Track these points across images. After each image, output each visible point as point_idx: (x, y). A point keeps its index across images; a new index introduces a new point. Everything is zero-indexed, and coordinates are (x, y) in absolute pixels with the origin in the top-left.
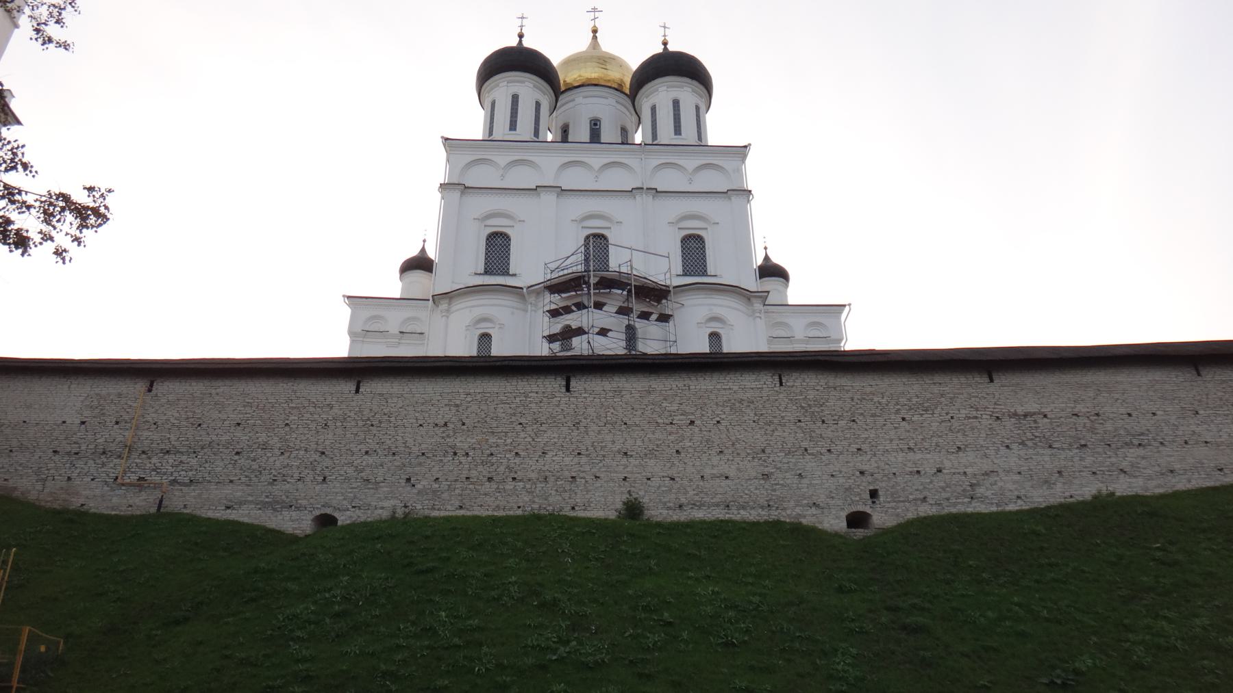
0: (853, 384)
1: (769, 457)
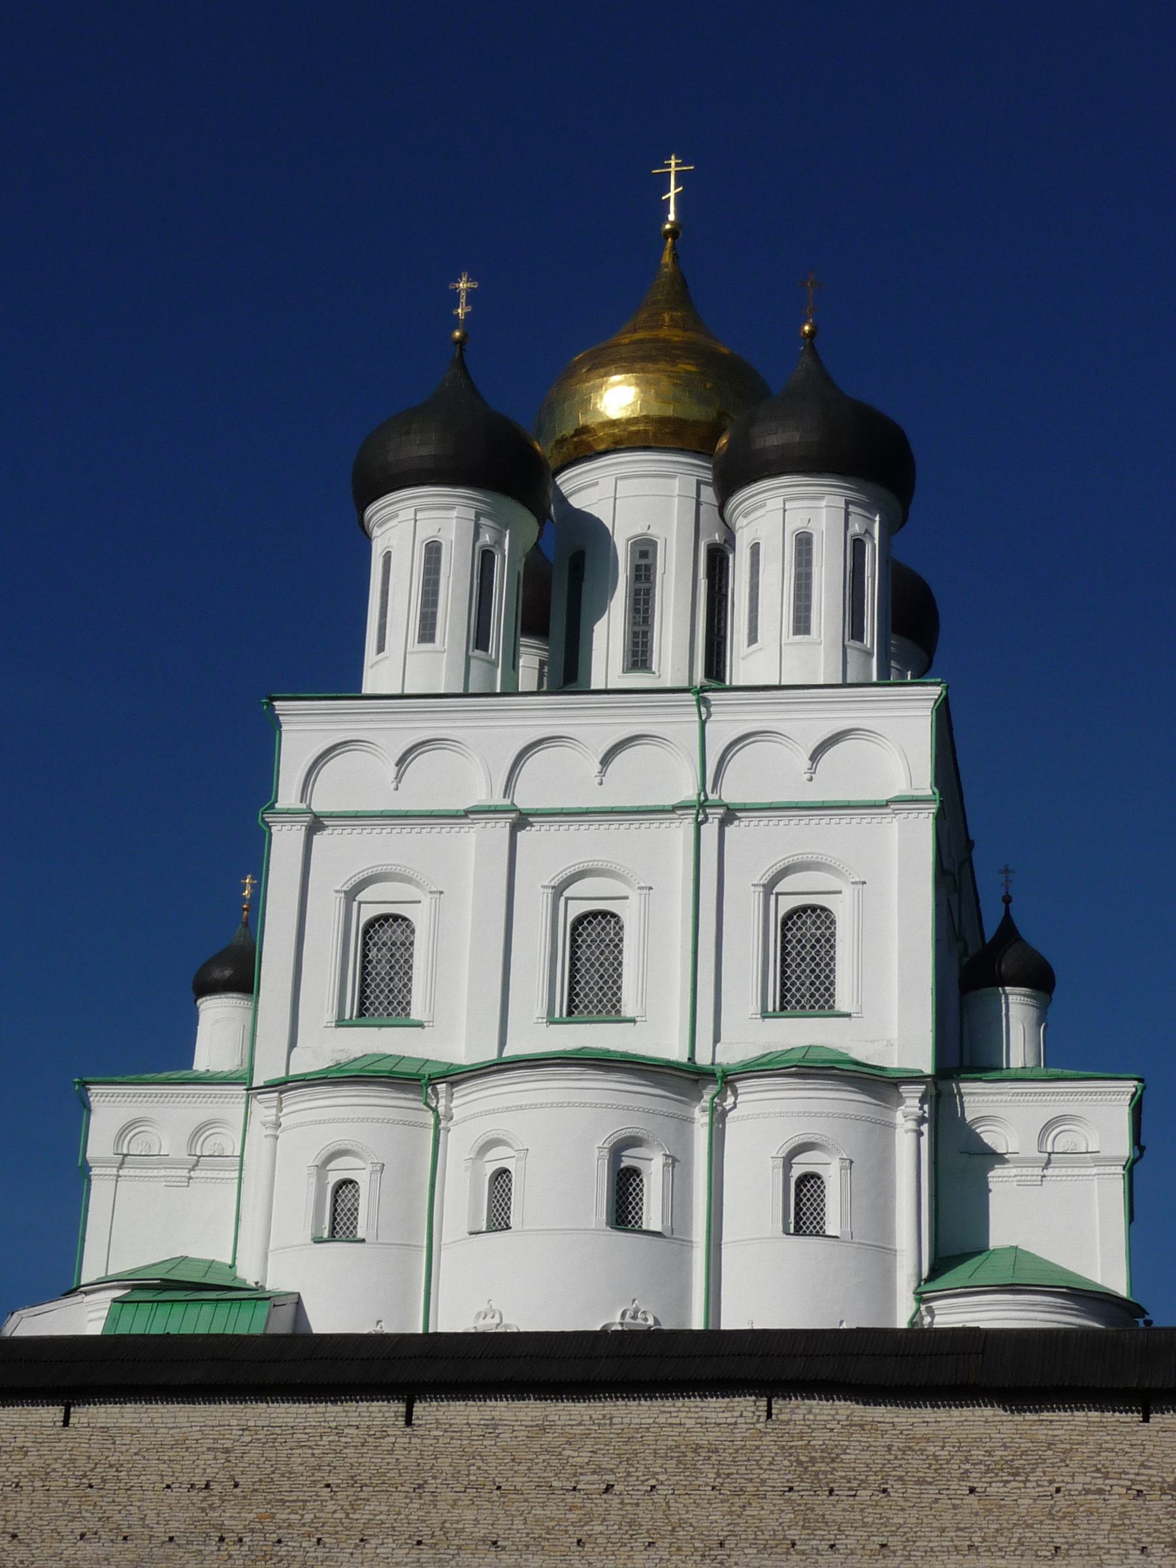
1: (729, 1556)
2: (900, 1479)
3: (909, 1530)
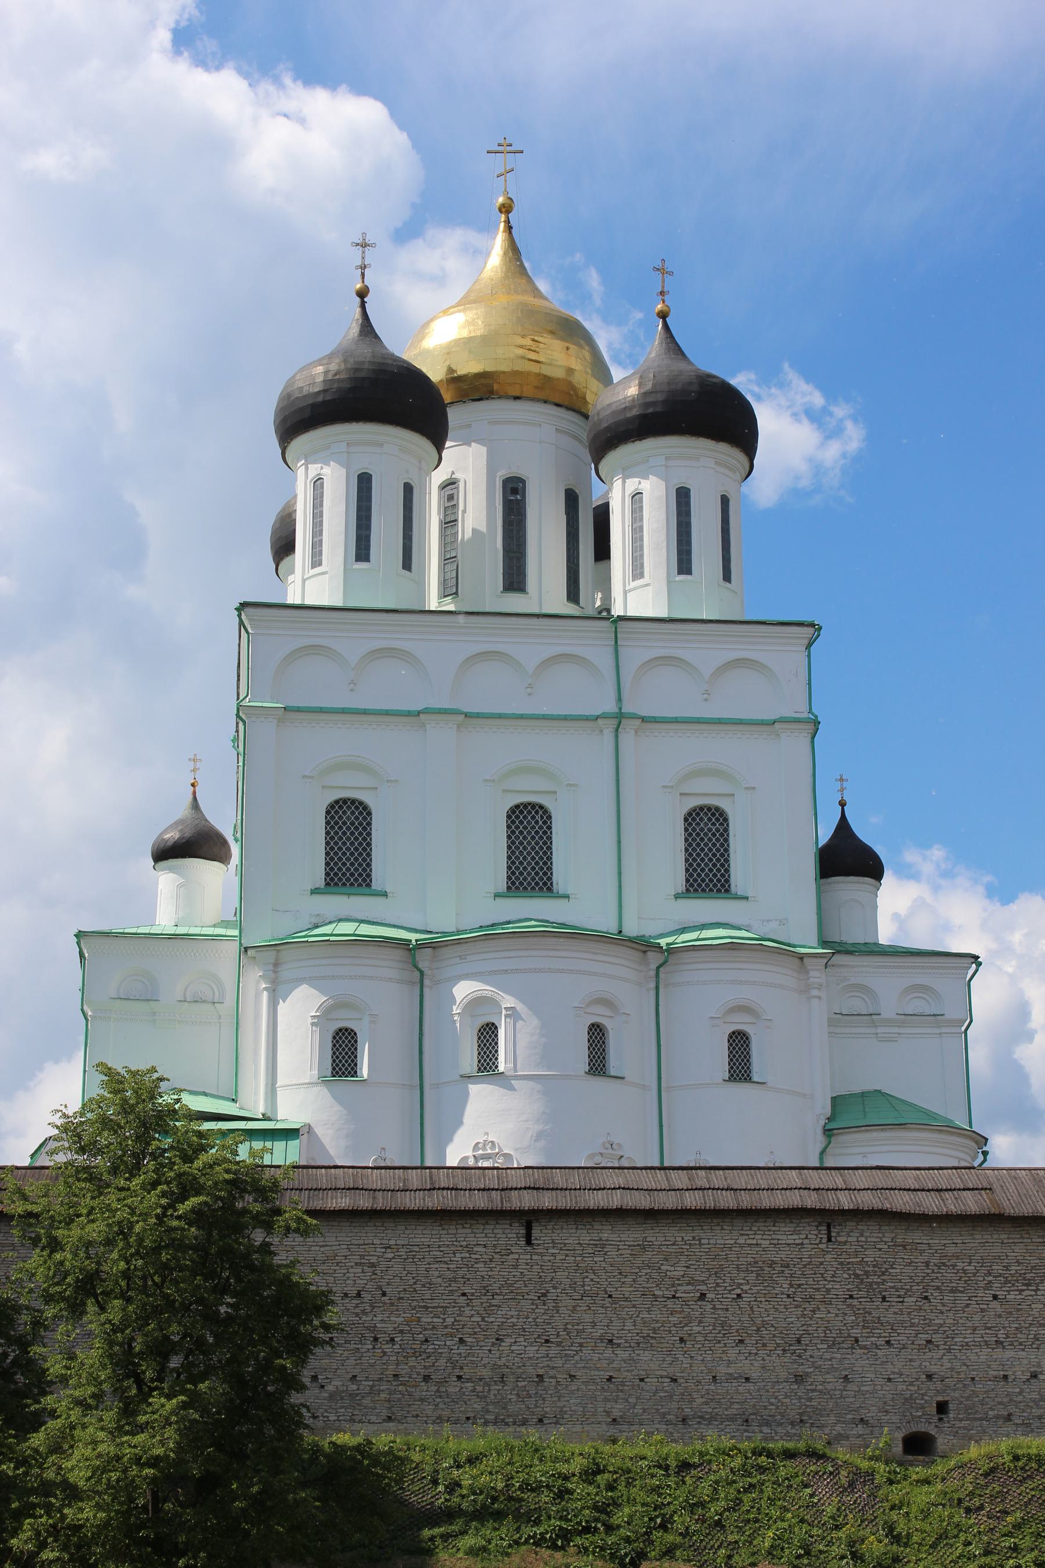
0: (931, 1241)
1: (805, 1350)
3: (948, 1329)
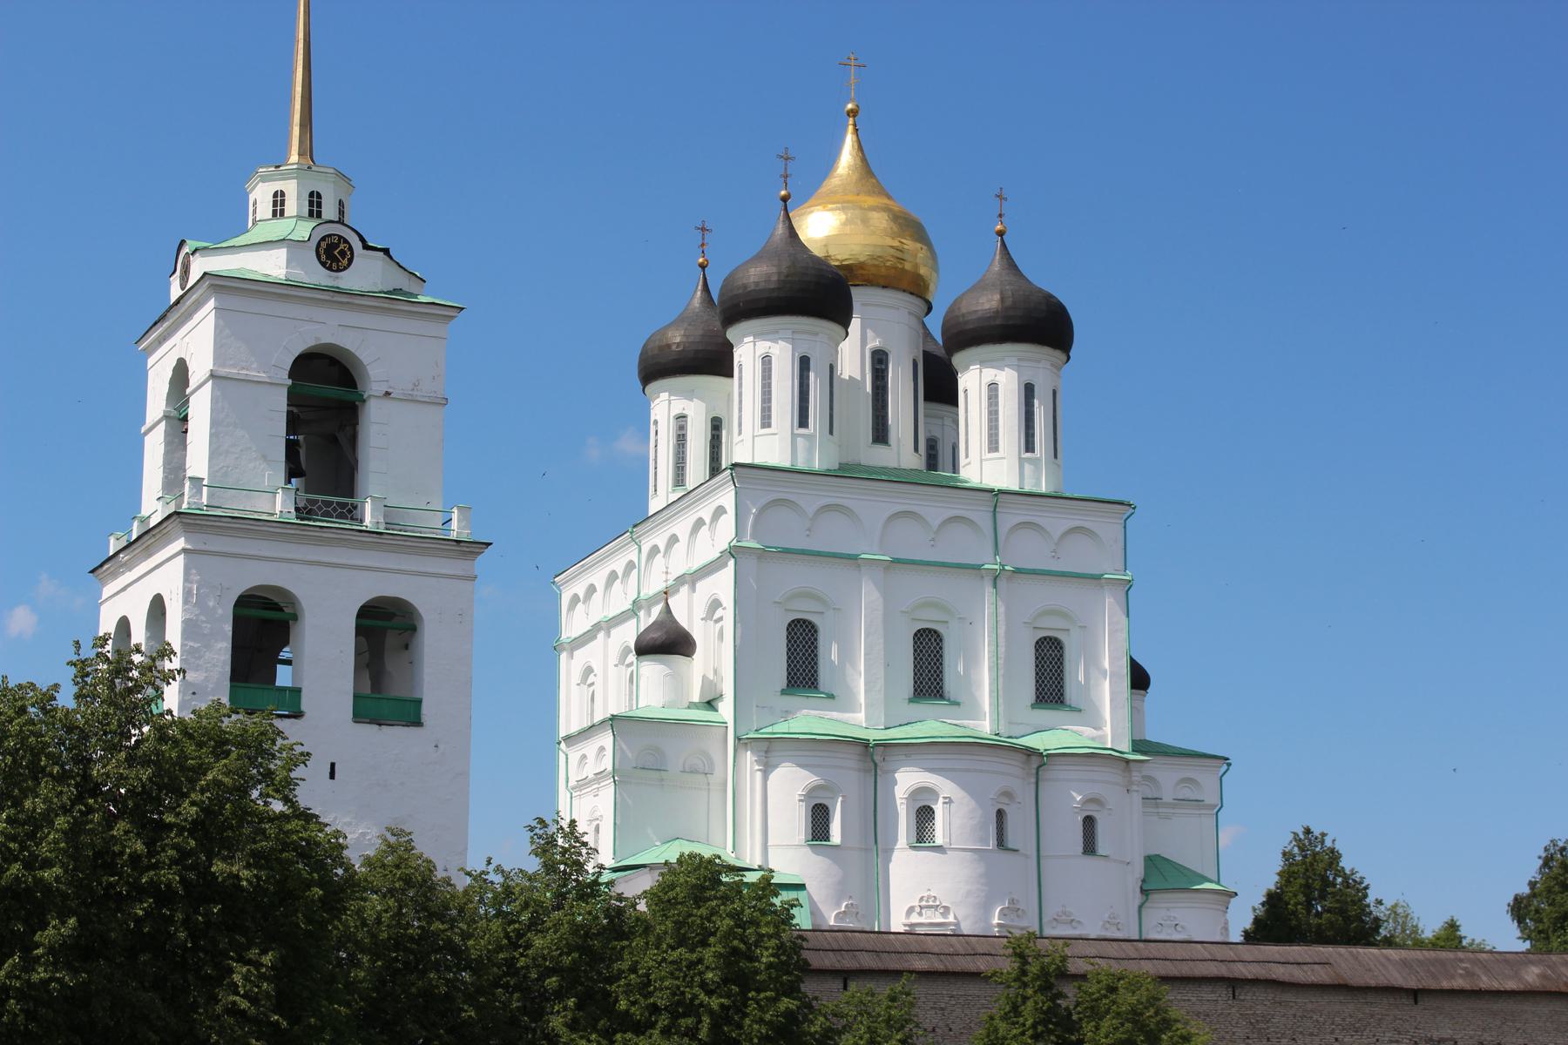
2: (1301, 1033)
